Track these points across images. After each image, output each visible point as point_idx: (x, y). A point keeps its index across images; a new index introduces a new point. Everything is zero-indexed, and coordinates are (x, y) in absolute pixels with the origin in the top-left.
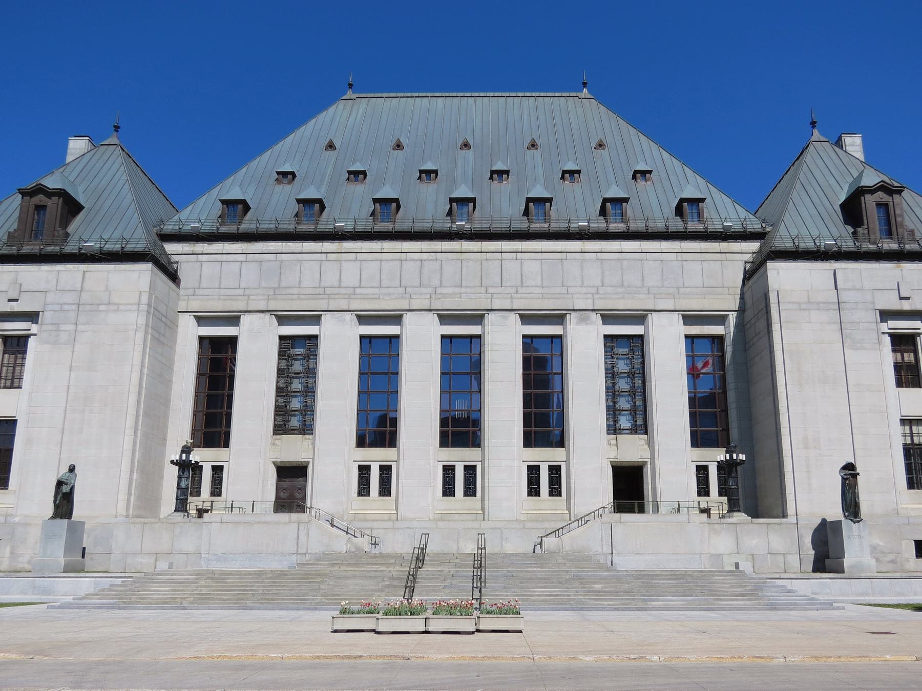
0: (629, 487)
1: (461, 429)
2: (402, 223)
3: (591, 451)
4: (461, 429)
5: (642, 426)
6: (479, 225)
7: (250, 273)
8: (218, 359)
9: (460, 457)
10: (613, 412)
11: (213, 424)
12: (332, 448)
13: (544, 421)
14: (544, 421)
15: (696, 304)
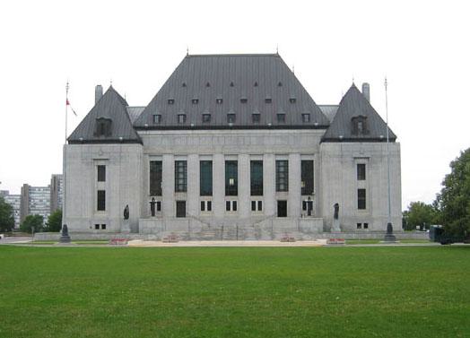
0: (282, 209)
1: (232, 190)
2: (212, 123)
3: (270, 198)
4: (232, 190)
5: (286, 189)
6: (237, 124)
7: (166, 142)
8: (156, 168)
9: (231, 199)
10: (278, 185)
11: (156, 189)
12: (193, 198)
13: (257, 188)
14: (257, 188)
15: (304, 151)
